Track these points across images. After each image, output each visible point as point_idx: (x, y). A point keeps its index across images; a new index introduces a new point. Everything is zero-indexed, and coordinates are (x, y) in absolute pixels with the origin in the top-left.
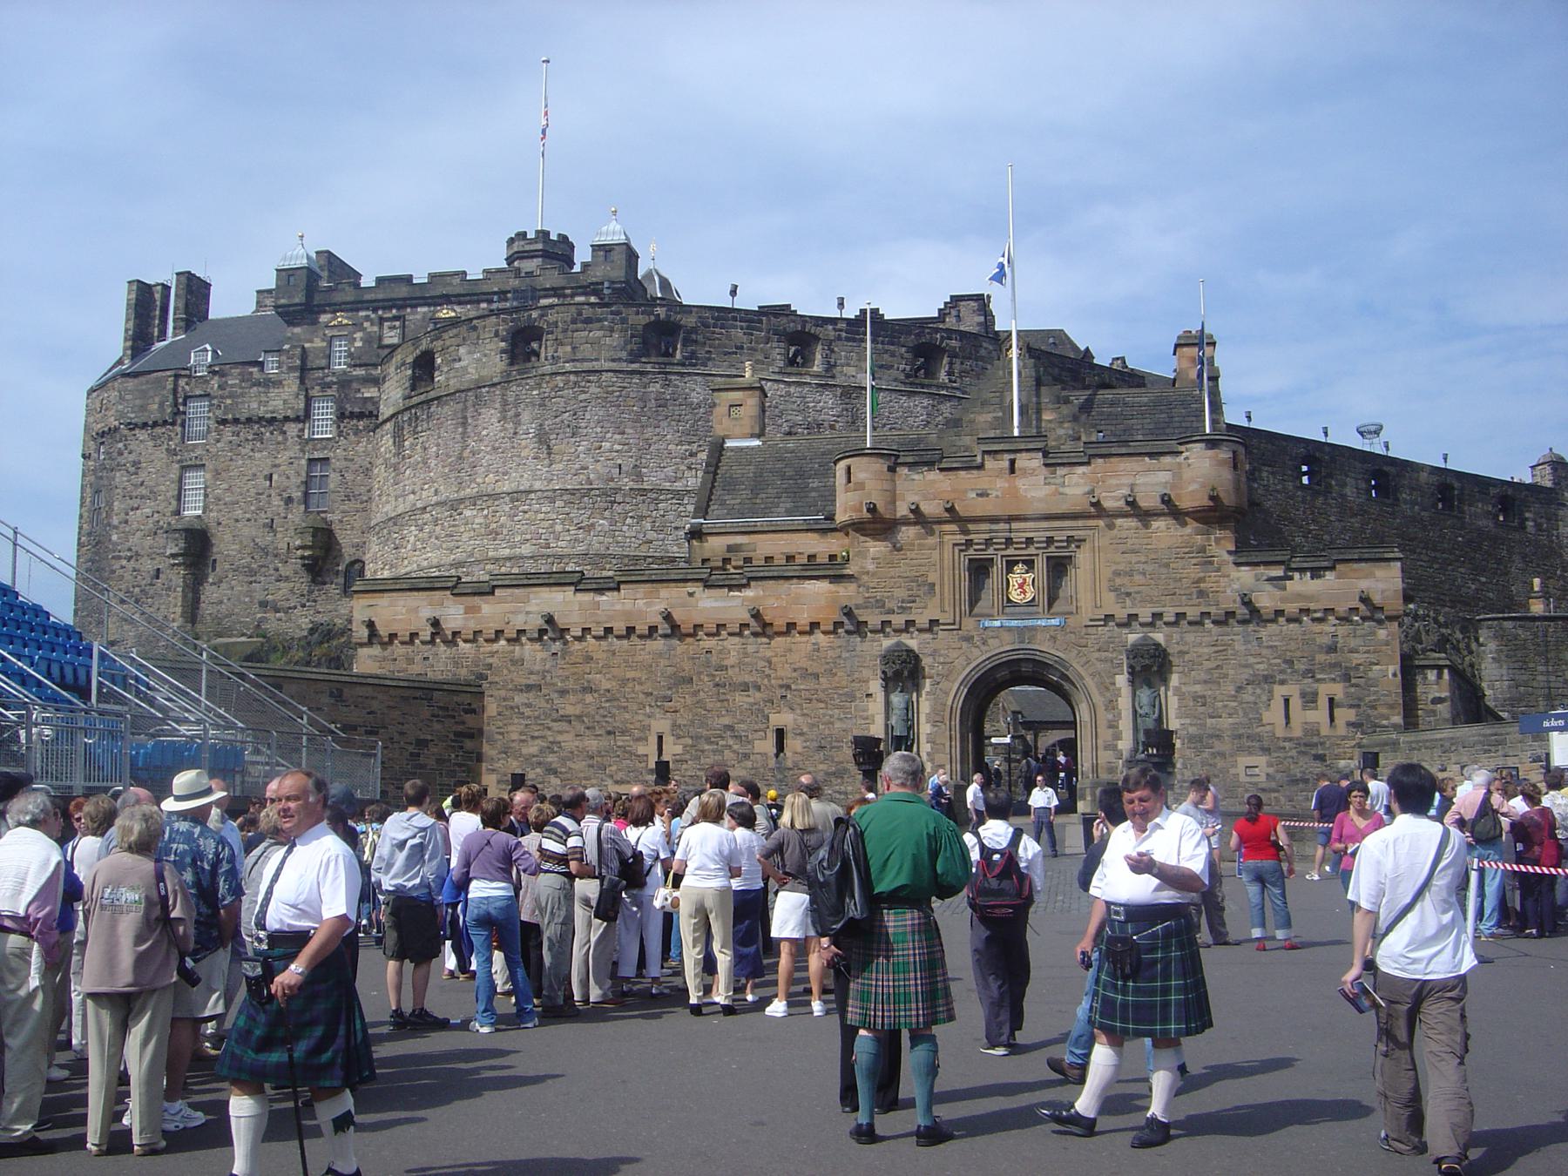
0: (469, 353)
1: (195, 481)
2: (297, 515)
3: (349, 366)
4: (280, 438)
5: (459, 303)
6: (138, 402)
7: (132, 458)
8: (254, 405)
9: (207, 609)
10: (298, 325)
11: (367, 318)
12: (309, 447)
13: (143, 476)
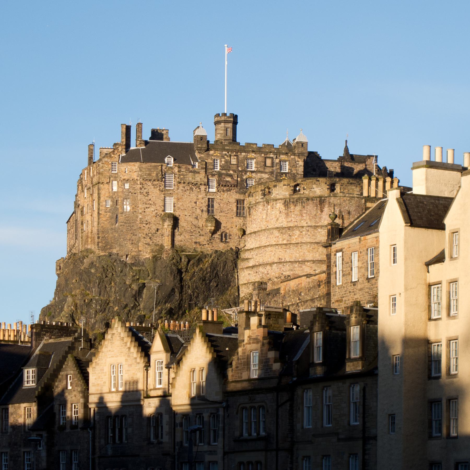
0: (317, 187)
1: (170, 201)
3: (220, 169)
4: (199, 190)
5: (255, 154)
6: (147, 172)
7: (146, 191)
8: (191, 179)
9: (177, 243)
10: (202, 154)
11: (226, 154)
12: (208, 194)
13: (150, 197)
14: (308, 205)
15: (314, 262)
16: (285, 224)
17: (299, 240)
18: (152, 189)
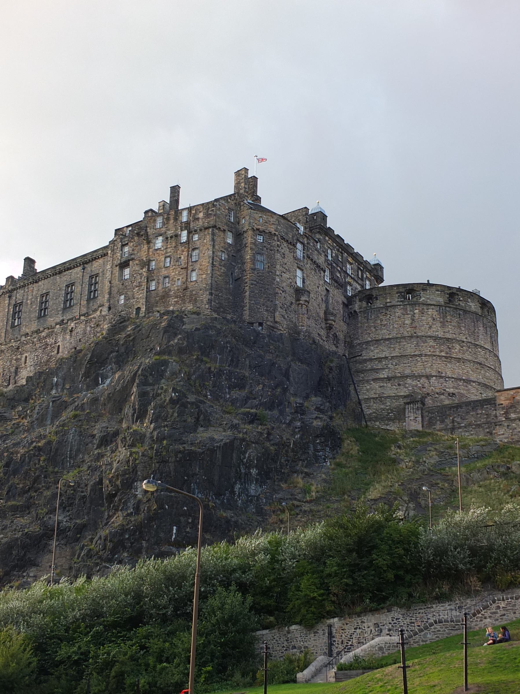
2: (324, 306)
7: (283, 251)
10: (321, 235)
13: (285, 261)
14: (465, 319)
15: (479, 384)
16: (440, 334)
17: (460, 356)
18: (288, 252)
